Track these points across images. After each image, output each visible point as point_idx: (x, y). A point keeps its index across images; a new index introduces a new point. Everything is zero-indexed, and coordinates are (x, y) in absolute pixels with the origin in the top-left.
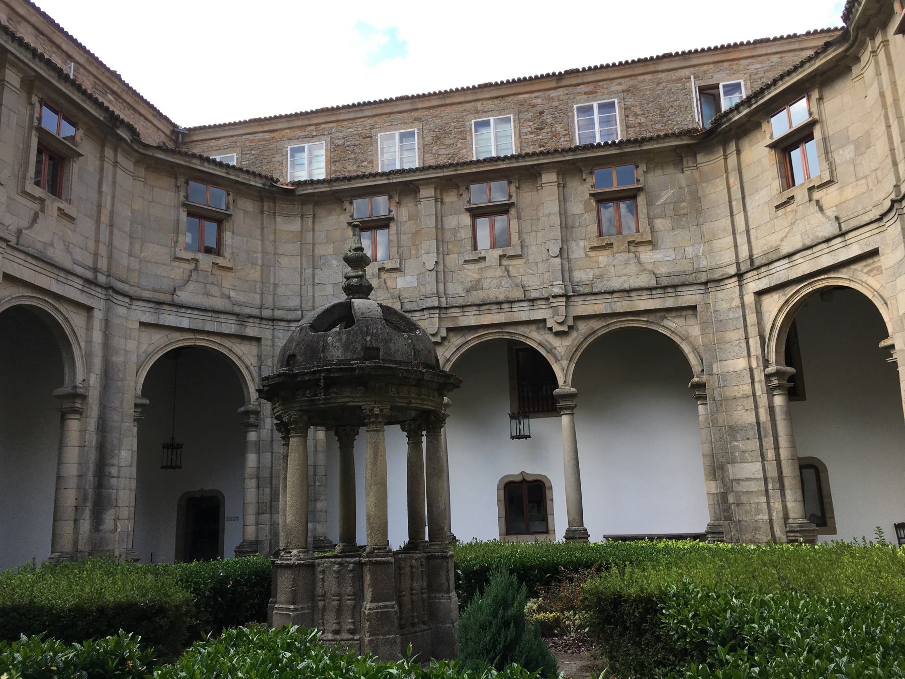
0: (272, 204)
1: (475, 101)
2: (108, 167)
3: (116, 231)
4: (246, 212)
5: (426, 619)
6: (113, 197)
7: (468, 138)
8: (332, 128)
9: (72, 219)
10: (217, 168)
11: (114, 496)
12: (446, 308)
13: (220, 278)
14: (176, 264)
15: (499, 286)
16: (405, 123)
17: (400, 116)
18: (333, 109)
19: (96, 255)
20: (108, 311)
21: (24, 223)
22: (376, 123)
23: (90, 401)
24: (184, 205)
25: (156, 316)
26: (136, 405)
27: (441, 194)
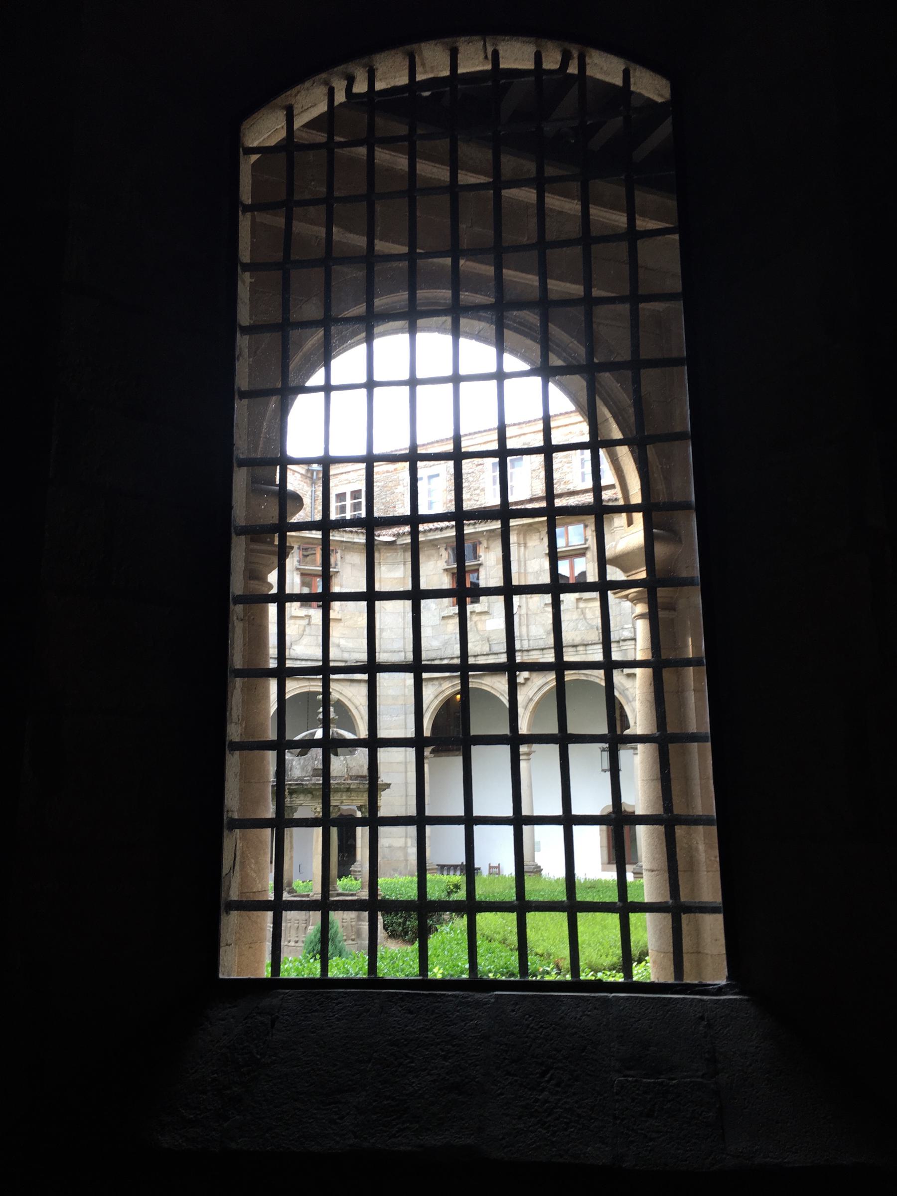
4: (353, 565)
5: (353, 937)
12: (528, 651)
15: (575, 629)
24: (297, 569)
27: (525, 539)
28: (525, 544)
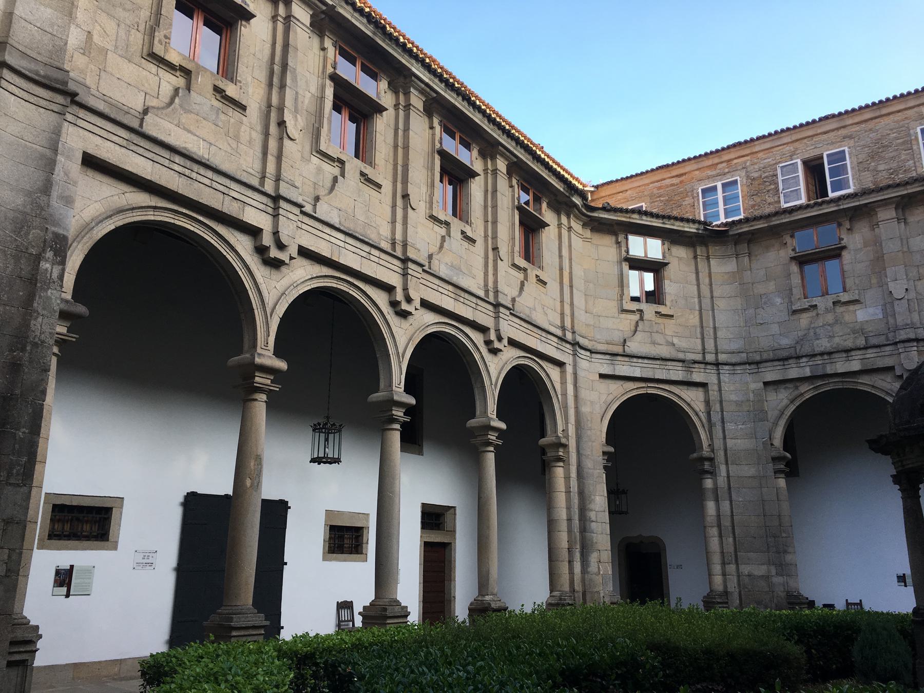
0: (704, 249)
1: (919, 105)
2: (565, 232)
3: (575, 291)
4: (680, 259)
6: (570, 259)
7: (915, 147)
8: (745, 162)
9: (545, 283)
10: (654, 220)
11: (595, 541)
13: (662, 327)
14: (623, 316)
16: (833, 143)
17: (825, 136)
18: (746, 142)
19: (562, 314)
20: (575, 366)
21: (515, 293)
22: (796, 149)
23: (570, 450)
25: (612, 367)
26: (604, 453)
27: (904, 215)
28: (905, 219)
